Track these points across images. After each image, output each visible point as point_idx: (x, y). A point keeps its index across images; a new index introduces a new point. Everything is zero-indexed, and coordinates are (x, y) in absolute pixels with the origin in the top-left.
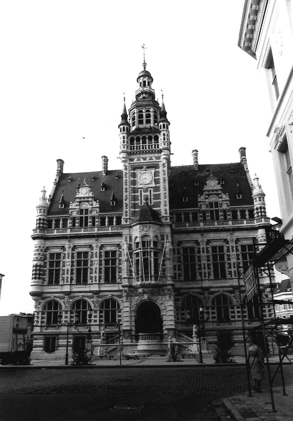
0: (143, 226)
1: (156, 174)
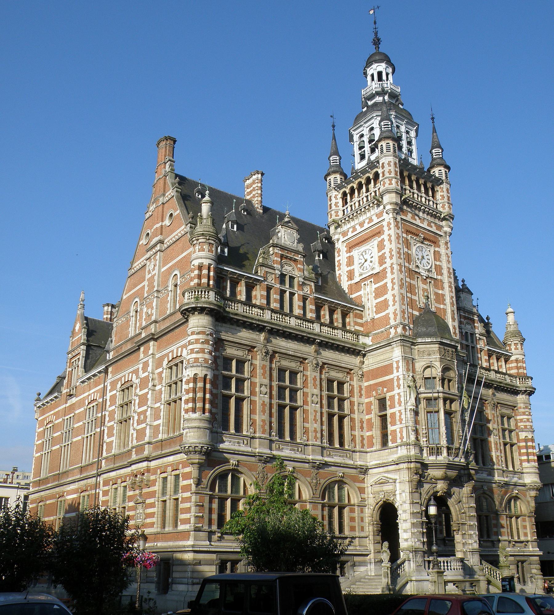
0: (445, 349)
1: (437, 256)
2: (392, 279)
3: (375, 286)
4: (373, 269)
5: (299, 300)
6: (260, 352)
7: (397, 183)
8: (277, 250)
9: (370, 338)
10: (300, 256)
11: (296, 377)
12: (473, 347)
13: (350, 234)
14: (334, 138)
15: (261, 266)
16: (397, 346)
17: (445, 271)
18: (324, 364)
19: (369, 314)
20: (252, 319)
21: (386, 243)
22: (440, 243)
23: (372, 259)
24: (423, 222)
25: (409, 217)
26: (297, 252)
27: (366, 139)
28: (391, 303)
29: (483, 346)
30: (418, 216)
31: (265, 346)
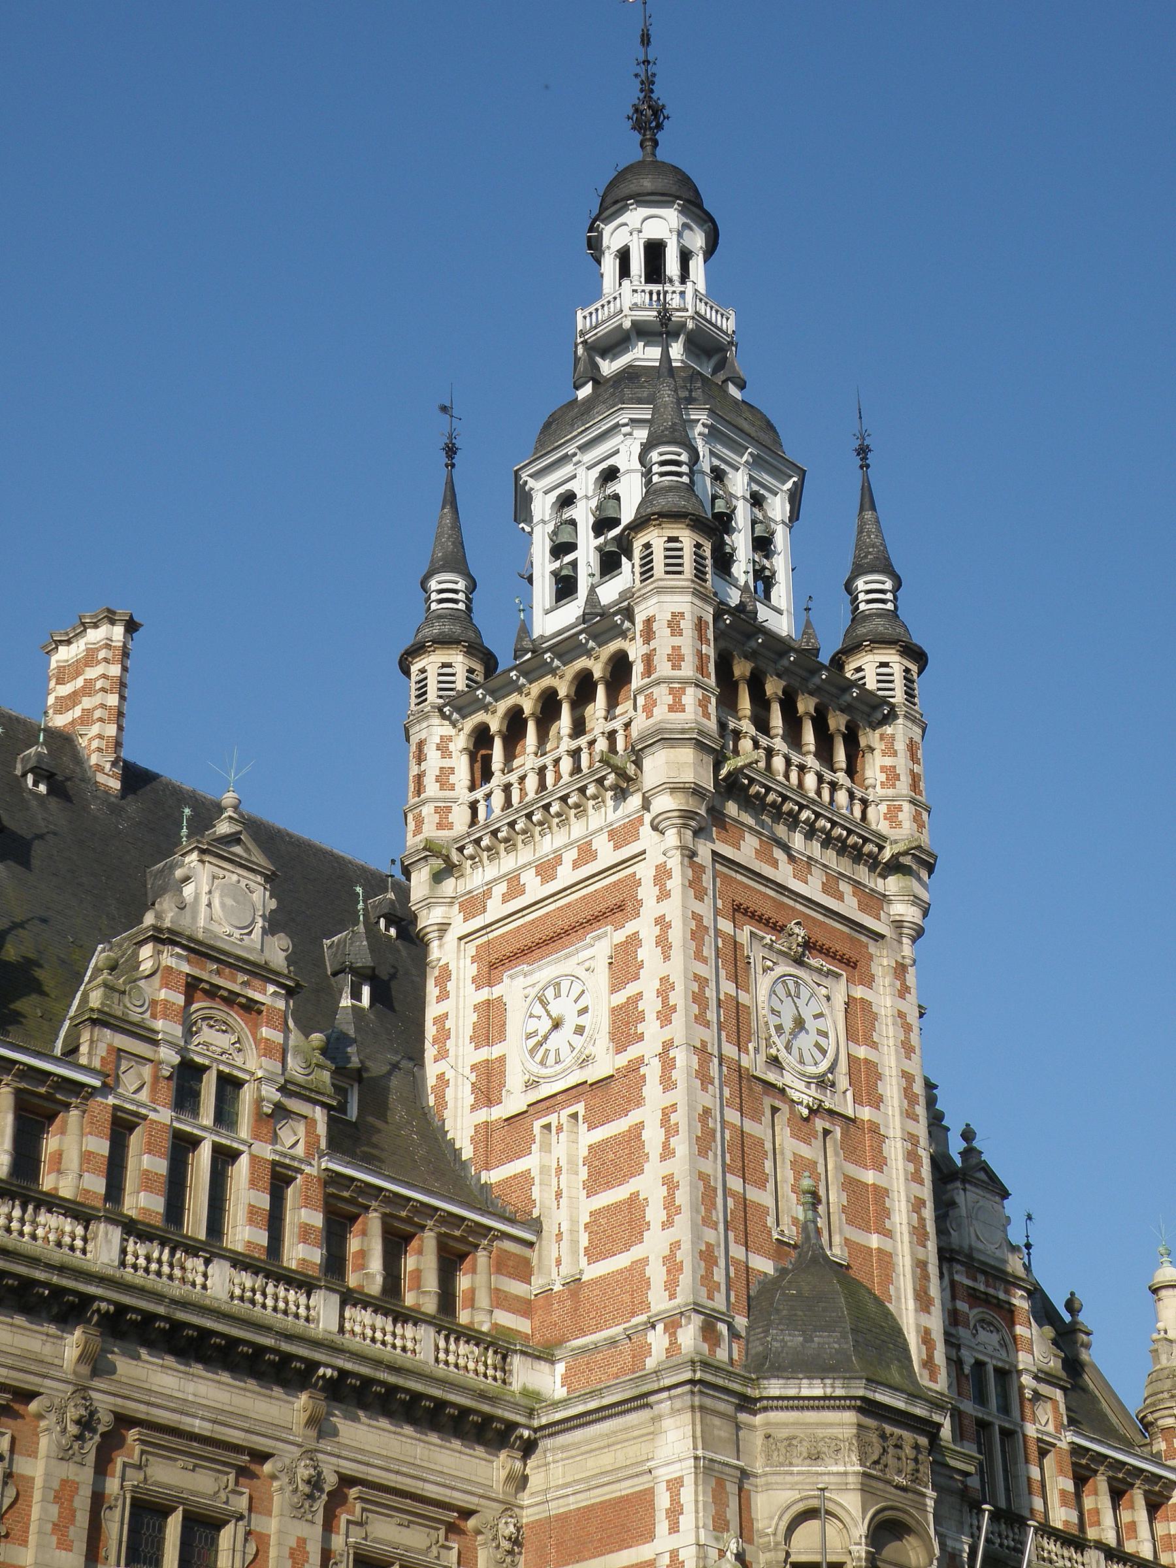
0: (883, 1436)
2: (663, 1109)
3: (589, 1137)
4: (585, 1061)
5: (253, 1184)
6: (53, 1417)
7: (703, 704)
8: (170, 958)
9: (560, 1368)
10: (271, 989)
11: (214, 1542)
12: (1008, 1435)
13: (495, 908)
14: (451, 499)
15: (94, 1022)
16: (675, 1412)
17: (891, 1089)
18: (347, 1481)
19: (561, 1259)
20: (34, 1261)
21: (647, 953)
22: (877, 970)
23: (584, 1020)
24: (806, 875)
25: (747, 851)
26: (260, 972)
27: (583, 514)
28: (655, 1214)
29: (1051, 1428)
30: (786, 848)
31: (82, 1390)
